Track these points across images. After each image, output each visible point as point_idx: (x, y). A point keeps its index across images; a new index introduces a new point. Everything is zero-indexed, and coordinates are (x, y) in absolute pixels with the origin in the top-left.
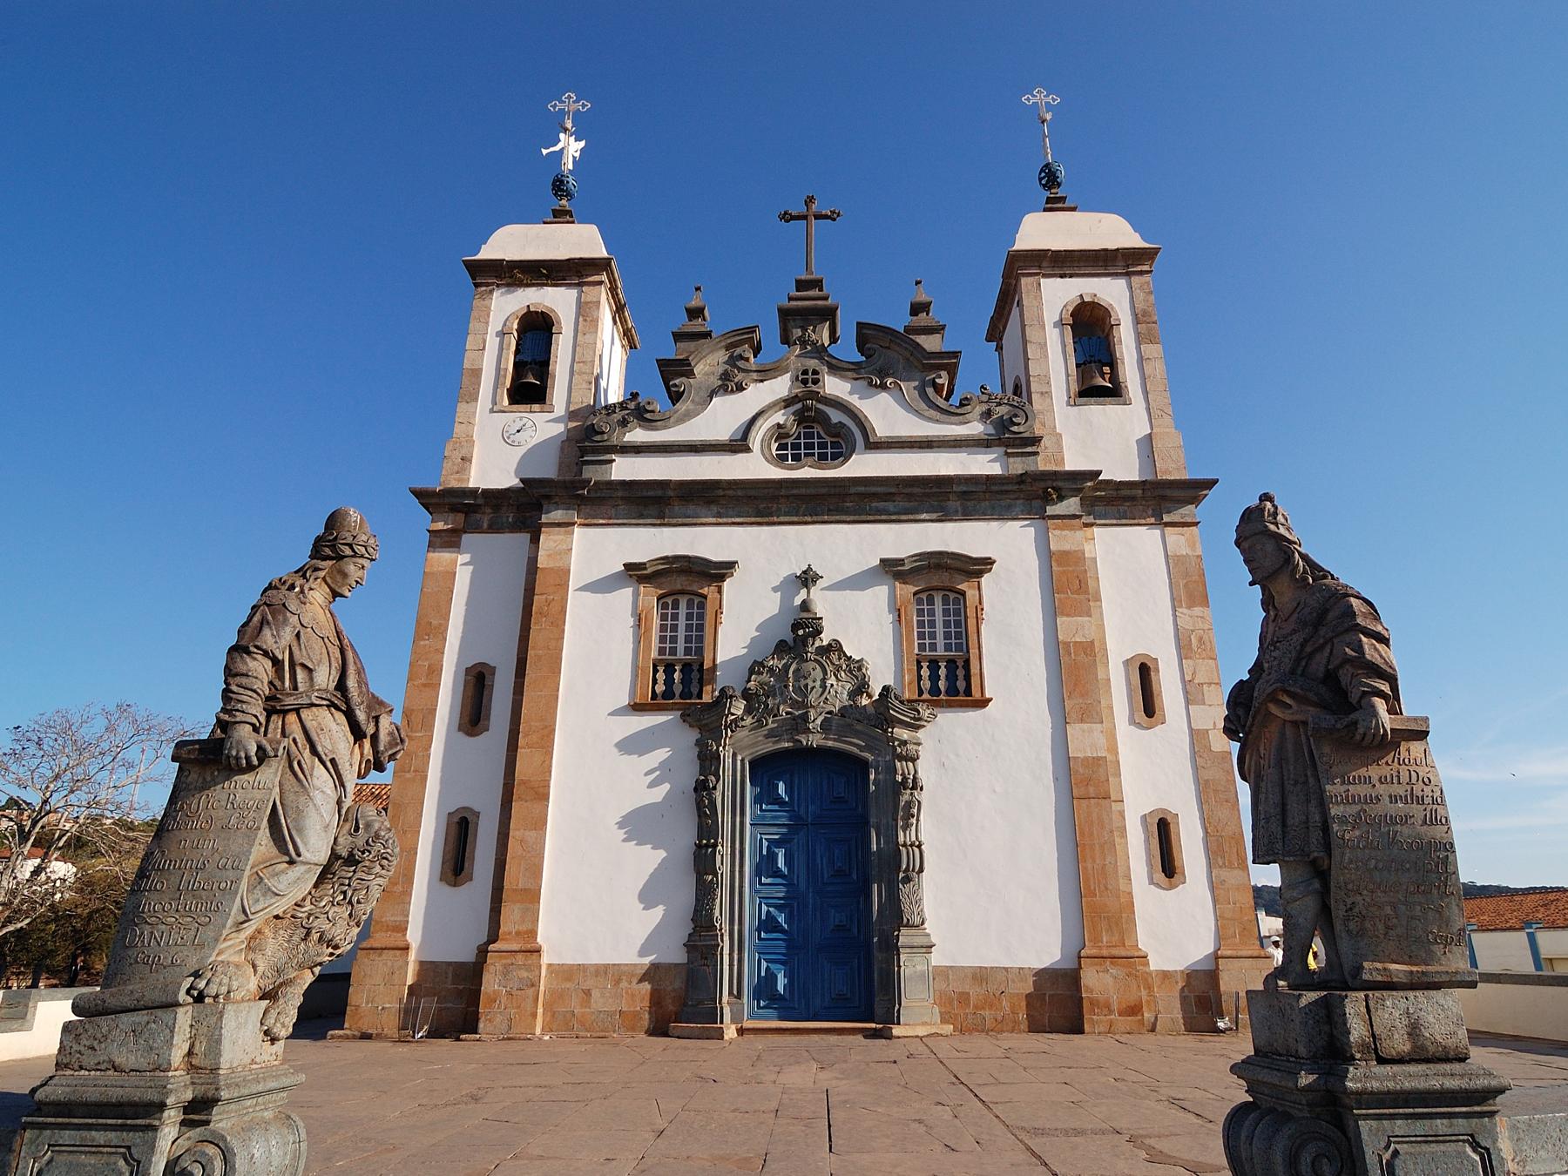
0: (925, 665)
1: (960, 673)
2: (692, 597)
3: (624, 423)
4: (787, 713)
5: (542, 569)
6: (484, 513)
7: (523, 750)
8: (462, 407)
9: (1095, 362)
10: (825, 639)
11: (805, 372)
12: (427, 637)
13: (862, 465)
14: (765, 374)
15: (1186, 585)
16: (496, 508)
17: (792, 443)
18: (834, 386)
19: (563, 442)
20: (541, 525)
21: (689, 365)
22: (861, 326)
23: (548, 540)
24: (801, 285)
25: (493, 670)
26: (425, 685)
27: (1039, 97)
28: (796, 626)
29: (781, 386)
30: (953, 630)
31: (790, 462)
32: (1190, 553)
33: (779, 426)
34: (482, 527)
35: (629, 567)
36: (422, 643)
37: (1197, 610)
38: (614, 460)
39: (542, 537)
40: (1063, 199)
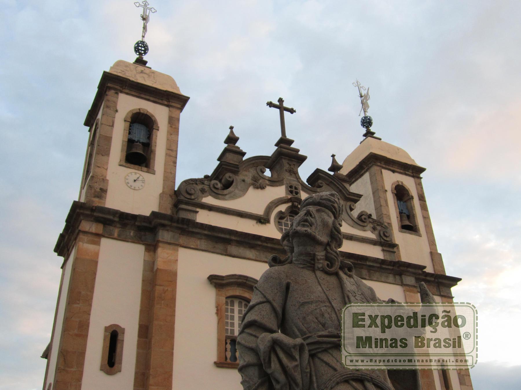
2: (241, 300)
3: (203, 191)
5: (161, 270)
6: (115, 226)
7: (152, 387)
11: (291, 187)
12: (78, 302)
14: (273, 182)
16: (124, 226)
17: (284, 223)
19: (160, 194)
20: (158, 241)
21: (238, 168)
25: (123, 331)
26: (77, 335)
33: (281, 212)
34: (113, 235)
36: (75, 305)
38: (197, 212)
39: (160, 250)
40: (374, 133)
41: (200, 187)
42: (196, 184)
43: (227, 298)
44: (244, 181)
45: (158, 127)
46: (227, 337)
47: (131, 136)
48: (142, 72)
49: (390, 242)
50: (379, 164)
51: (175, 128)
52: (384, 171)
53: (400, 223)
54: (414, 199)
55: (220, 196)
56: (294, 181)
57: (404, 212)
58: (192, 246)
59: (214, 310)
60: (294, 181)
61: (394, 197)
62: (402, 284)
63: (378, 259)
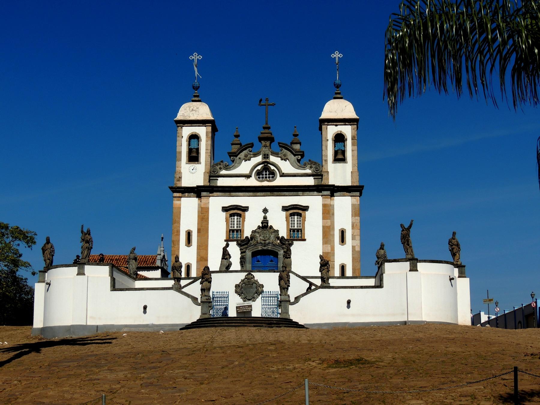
0: (292, 231)
1: (300, 233)
3: (220, 168)
4: (260, 242)
8: (177, 163)
9: (340, 150)
10: (269, 225)
11: (265, 155)
13: (279, 181)
14: (255, 155)
15: (354, 211)
18: (273, 159)
21: (236, 154)
22: (279, 143)
23: (204, 200)
24: (264, 128)
26: (177, 235)
27: (337, 55)
28: (262, 223)
29: (259, 159)
30: (299, 222)
31: (261, 179)
32: (357, 203)
33: (258, 170)
34: (186, 196)
35: (223, 208)
36: (175, 225)
37: (357, 218)
38: (218, 180)
41: (219, 166)
42: (218, 166)
43: (230, 215)
44: (240, 158)
45: (201, 140)
46: (230, 230)
47: (190, 147)
48: (193, 110)
49: (319, 173)
50: (326, 123)
51: (209, 137)
52: (328, 127)
53: (334, 158)
54: (347, 141)
55: (228, 169)
56: (267, 151)
57: (340, 149)
58: (216, 195)
59: (225, 220)
60: (267, 151)
61: (333, 142)
62: (322, 196)
63: (305, 185)
